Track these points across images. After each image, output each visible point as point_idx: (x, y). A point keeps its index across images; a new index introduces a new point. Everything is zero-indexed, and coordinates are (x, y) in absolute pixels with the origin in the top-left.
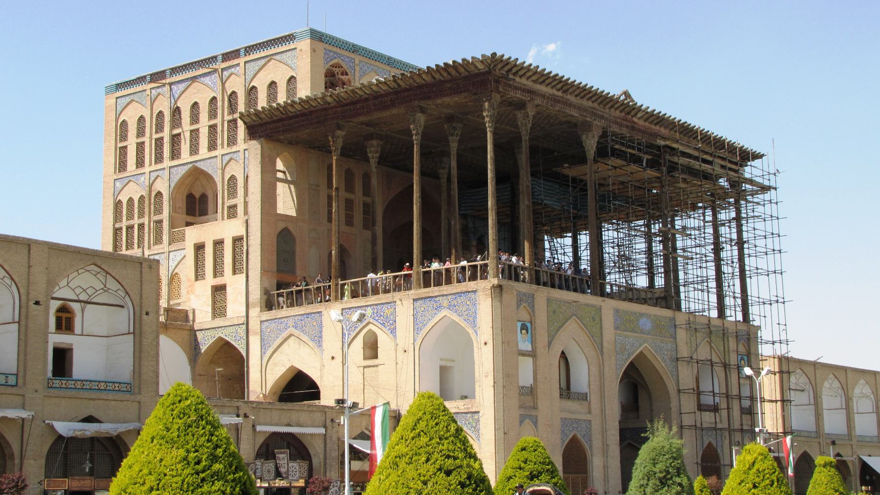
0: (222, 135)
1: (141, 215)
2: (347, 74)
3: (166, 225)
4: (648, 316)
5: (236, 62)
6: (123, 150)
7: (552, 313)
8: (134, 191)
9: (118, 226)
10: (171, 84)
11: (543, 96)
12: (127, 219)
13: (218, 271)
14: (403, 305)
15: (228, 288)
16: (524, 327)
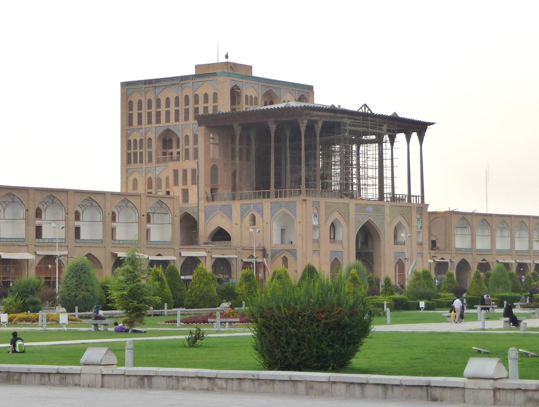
0: (182, 116)
1: (141, 147)
2: (239, 89)
3: (154, 154)
4: (371, 205)
5: (188, 81)
6: (131, 116)
7: (327, 208)
8: (136, 136)
9: (129, 152)
10: (155, 87)
11: (325, 116)
12: (134, 149)
13: (185, 182)
14: (267, 204)
15: (189, 191)
16: (315, 216)
